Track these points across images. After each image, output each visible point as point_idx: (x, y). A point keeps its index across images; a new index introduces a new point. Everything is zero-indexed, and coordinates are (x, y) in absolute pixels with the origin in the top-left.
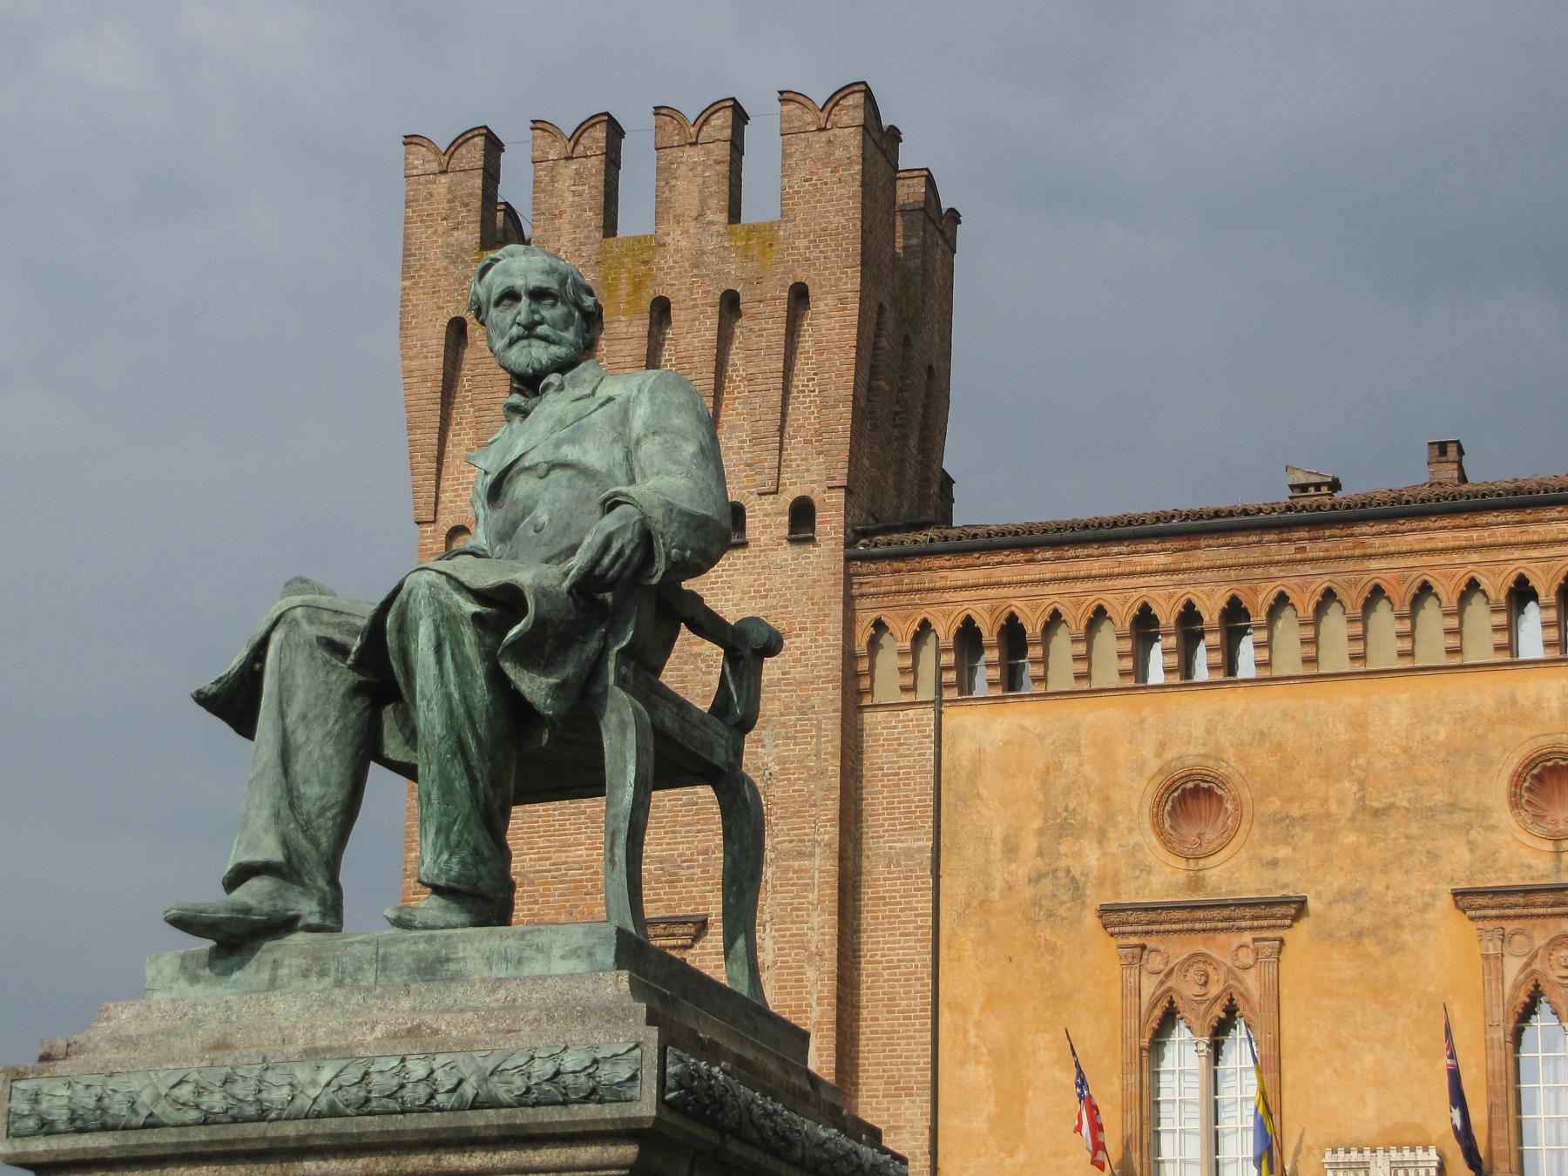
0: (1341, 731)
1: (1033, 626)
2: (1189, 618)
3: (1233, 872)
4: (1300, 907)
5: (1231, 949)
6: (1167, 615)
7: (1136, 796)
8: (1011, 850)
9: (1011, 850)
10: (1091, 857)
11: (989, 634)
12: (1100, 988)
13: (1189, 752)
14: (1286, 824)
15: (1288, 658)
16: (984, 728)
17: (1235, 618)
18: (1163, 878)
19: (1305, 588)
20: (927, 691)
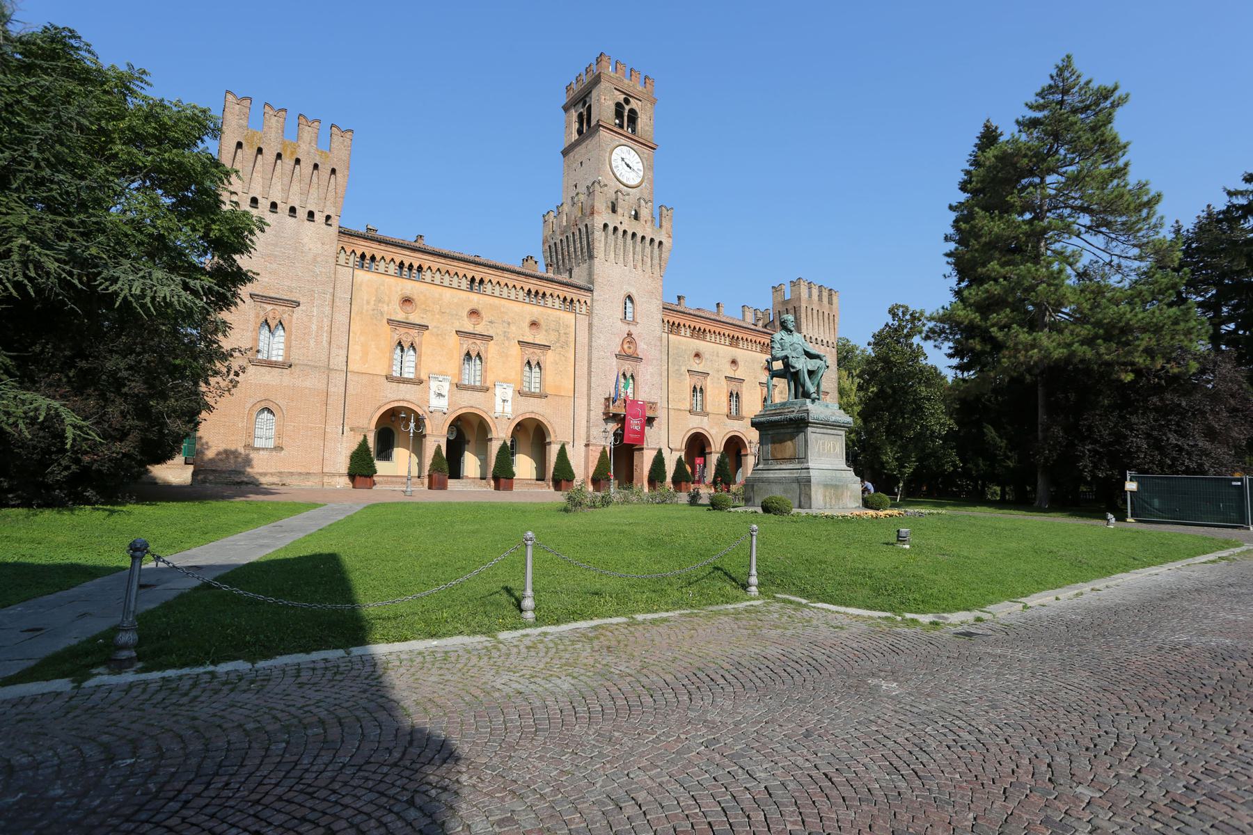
0: (437, 295)
1: (378, 258)
2: (411, 266)
3: (414, 318)
4: (426, 327)
5: (414, 332)
6: (407, 265)
7: (396, 299)
8: (368, 303)
9: (368, 303)
10: (386, 308)
11: (368, 257)
12: (389, 335)
13: (408, 293)
14: (425, 311)
15: (428, 279)
16: (361, 275)
17: (420, 268)
18: (400, 316)
19: (435, 267)
20: (351, 264)
